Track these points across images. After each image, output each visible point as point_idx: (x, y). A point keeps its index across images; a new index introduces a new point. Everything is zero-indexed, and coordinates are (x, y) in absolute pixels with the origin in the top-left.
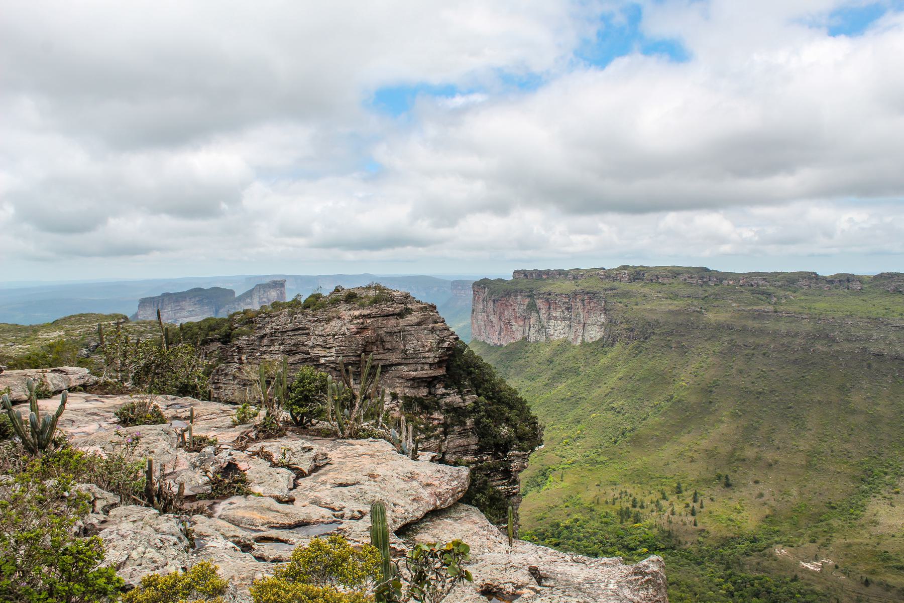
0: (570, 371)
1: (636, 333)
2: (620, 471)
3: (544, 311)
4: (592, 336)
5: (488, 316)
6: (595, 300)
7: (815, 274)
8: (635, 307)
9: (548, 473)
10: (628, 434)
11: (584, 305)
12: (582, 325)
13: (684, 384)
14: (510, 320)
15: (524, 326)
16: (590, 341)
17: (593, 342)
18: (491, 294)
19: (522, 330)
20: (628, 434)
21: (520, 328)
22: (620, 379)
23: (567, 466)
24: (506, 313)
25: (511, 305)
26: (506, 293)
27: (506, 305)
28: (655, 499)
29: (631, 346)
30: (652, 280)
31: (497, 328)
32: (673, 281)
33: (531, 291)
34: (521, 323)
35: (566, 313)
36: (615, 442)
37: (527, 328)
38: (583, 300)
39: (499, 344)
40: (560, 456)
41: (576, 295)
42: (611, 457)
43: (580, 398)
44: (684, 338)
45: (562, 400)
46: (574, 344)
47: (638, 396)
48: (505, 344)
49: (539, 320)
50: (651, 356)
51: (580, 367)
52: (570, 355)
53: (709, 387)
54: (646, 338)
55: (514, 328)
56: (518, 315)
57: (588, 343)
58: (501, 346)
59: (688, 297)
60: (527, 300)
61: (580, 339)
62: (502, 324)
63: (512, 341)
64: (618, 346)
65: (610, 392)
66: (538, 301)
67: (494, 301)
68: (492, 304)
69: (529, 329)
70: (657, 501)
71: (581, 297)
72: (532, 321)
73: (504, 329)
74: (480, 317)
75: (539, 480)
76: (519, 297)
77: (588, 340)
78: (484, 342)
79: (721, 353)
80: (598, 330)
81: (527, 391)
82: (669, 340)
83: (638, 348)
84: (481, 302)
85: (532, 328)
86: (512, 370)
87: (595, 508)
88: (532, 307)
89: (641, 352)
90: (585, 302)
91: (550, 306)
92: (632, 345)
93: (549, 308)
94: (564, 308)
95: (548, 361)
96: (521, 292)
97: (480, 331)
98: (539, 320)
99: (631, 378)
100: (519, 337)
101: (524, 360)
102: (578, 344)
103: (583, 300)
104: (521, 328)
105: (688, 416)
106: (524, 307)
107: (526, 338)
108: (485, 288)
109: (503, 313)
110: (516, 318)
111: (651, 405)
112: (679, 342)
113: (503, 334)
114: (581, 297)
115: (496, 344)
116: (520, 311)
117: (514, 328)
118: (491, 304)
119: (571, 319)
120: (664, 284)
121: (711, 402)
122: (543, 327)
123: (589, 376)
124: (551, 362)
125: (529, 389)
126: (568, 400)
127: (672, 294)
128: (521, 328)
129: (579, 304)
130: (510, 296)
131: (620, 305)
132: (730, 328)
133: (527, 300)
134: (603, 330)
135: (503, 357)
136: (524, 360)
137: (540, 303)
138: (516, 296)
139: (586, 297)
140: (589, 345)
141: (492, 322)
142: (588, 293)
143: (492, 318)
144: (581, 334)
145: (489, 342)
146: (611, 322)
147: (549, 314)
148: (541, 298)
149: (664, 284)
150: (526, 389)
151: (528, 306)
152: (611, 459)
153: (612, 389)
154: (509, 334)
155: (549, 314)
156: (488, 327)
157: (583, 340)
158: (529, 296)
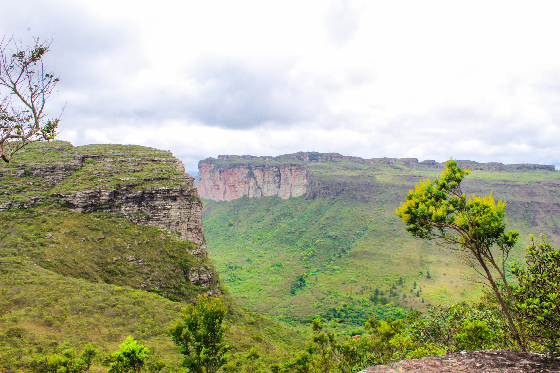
0: (286, 216)
1: (331, 190)
2: (353, 274)
3: (260, 178)
4: (298, 193)
5: (215, 182)
6: (299, 170)
7: (417, 159)
8: (327, 174)
9: (304, 278)
10: (347, 251)
11: (292, 173)
12: (290, 186)
13: (373, 220)
14: (234, 184)
15: (245, 188)
16: (296, 196)
17: (299, 197)
18: (218, 167)
19: (243, 190)
20: (347, 251)
21: (242, 189)
22: (328, 218)
23: (314, 273)
24: (231, 179)
25: (235, 174)
26: (232, 166)
27: (231, 174)
28: (389, 289)
29: (328, 198)
30: (327, 159)
31: (222, 190)
32: (342, 160)
33: (249, 165)
34: (243, 186)
35: (276, 178)
36: (340, 257)
37: (247, 189)
38: (291, 170)
39: (223, 200)
40: (305, 267)
41: (285, 167)
42: (342, 266)
43: (302, 231)
44: (365, 192)
45: (289, 233)
46: (284, 198)
47: (344, 228)
48: (229, 199)
49: (256, 183)
50: (345, 204)
51: (292, 213)
52: (283, 205)
53: (390, 221)
54: (338, 193)
55: (237, 189)
56: (241, 180)
57: (294, 198)
58: (226, 201)
59: (355, 169)
60: (248, 170)
61: (288, 195)
62: (227, 187)
63: (236, 198)
64: (318, 199)
65: (323, 227)
66: (255, 171)
67: (220, 172)
68: (219, 175)
69: (249, 189)
70: (390, 290)
71: (290, 168)
72: (251, 184)
73: (229, 190)
74: (207, 183)
75: (299, 283)
76: (242, 169)
77: (294, 195)
78: (211, 200)
79: (392, 201)
80: (301, 189)
81: (259, 229)
82: (355, 194)
83: (334, 199)
84: (208, 173)
85: (251, 189)
86: (241, 216)
87: (352, 297)
88: (251, 175)
89: (336, 202)
90: (293, 171)
91: (264, 174)
92: (329, 198)
93: (264, 176)
94: (274, 176)
95: (266, 210)
96: (243, 165)
97: (207, 192)
98: (256, 183)
99: (334, 218)
100: (241, 195)
101: (248, 210)
102: (287, 198)
103: (291, 170)
104: (243, 189)
105: (382, 239)
106: (245, 175)
107: (246, 196)
108: (211, 164)
109: (229, 180)
110: (239, 182)
111: (355, 233)
112: (361, 195)
113: (227, 194)
114: (290, 168)
115: (221, 201)
116: (242, 177)
117: (237, 189)
118: (217, 174)
119: (280, 182)
120: (337, 162)
121: (395, 230)
122: (259, 188)
123: (303, 217)
124: (268, 210)
125: (260, 227)
126: (293, 233)
127: (344, 167)
128: (243, 189)
129: (288, 172)
130: (235, 168)
131: (316, 173)
132: (393, 186)
133: (248, 170)
134: (305, 189)
135: (232, 208)
136: (248, 210)
137: (257, 173)
138: (239, 168)
139: (293, 168)
140: (295, 199)
141: (218, 186)
142: (295, 165)
143: (219, 183)
144: (289, 192)
145: (215, 199)
146: (311, 183)
147: (264, 180)
148: (258, 169)
149: (337, 162)
150: (258, 227)
151: (248, 174)
152: (342, 267)
153: (324, 224)
154: (233, 193)
155: (264, 180)
156: (214, 190)
157: (291, 196)
158: (249, 168)
